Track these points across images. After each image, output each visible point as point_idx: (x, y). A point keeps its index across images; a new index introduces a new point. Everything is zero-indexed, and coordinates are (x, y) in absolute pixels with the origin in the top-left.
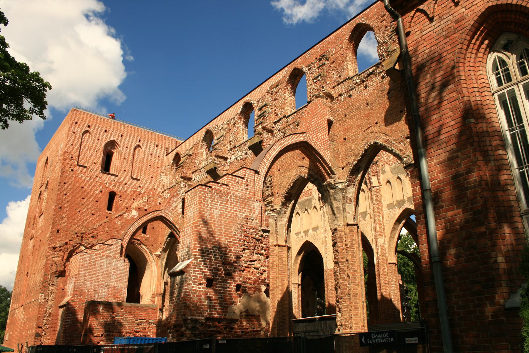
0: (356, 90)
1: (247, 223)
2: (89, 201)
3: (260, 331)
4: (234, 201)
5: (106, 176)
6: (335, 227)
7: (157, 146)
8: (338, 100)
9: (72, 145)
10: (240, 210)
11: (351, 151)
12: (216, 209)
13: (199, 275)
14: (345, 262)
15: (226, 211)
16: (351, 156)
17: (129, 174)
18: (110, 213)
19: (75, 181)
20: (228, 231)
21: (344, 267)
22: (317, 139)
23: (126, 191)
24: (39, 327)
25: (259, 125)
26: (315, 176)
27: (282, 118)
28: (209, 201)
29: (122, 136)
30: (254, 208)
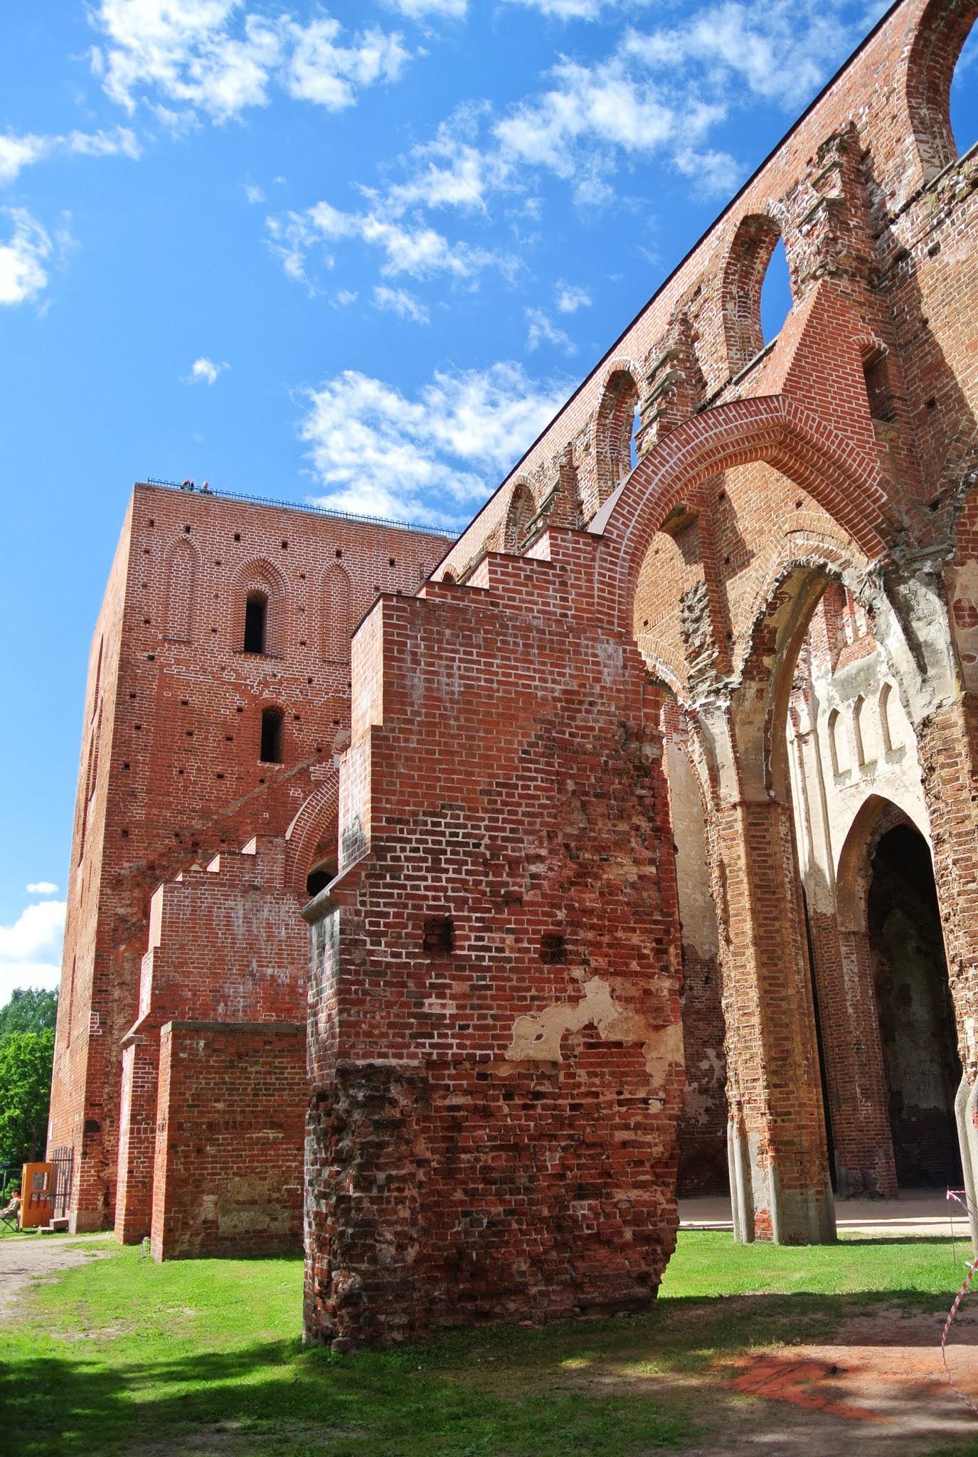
0: (953, 223)
1: (573, 718)
2: (206, 738)
3: (645, 1101)
4: (516, 644)
5: (254, 667)
6: (925, 715)
7: (392, 563)
8: (894, 276)
9: (145, 586)
10: (543, 672)
11: (958, 440)
12: (450, 676)
13: (392, 910)
14: (967, 833)
15: (486, 680)
16: (959, 457)
17: (315, 652)
18: (270, 770)
19: (160, 687)
20: (499, 749)
21: (969, 851)
22: (826, 415)
23: (310, 702)
24: (92, 1105)
25: (650, 424)
26: (843, 553)
27: (722, 390)
28: (422, 650)
29: (285, 545)
30: (597, 663)
